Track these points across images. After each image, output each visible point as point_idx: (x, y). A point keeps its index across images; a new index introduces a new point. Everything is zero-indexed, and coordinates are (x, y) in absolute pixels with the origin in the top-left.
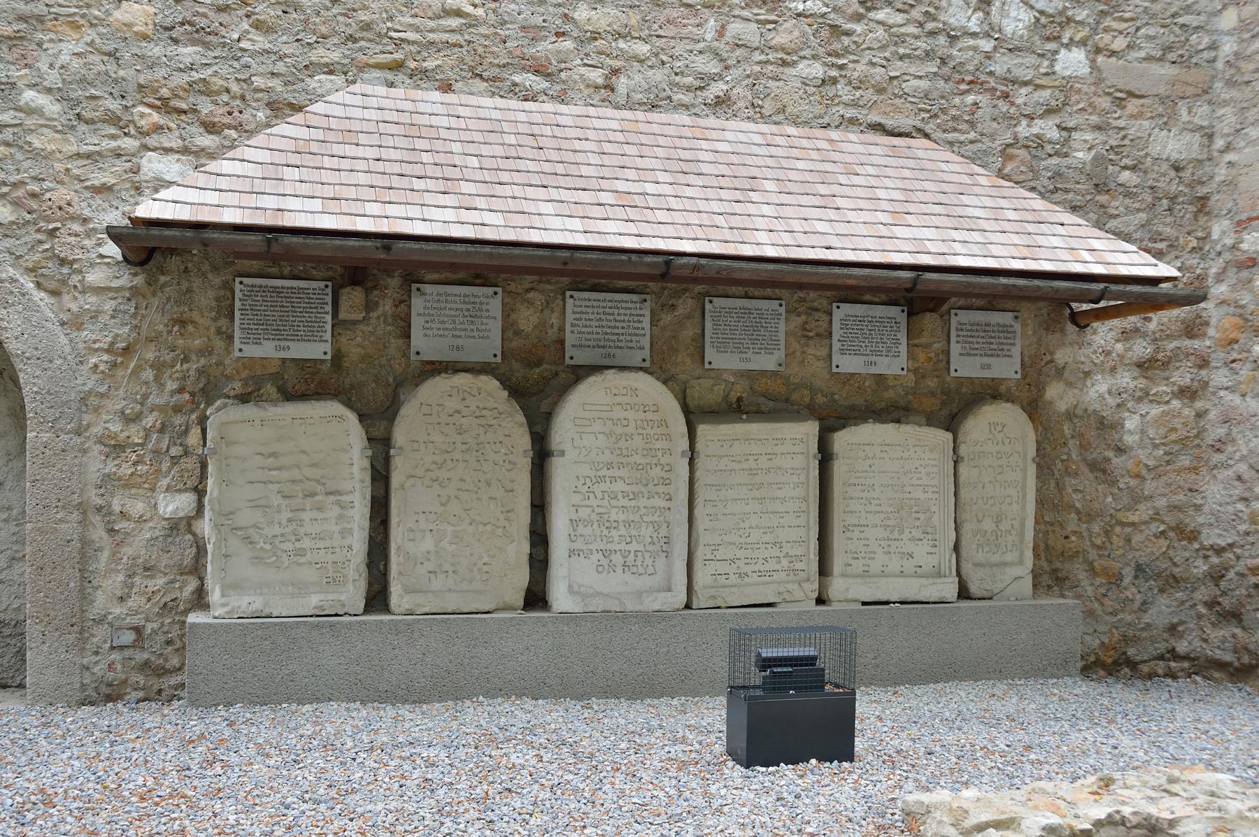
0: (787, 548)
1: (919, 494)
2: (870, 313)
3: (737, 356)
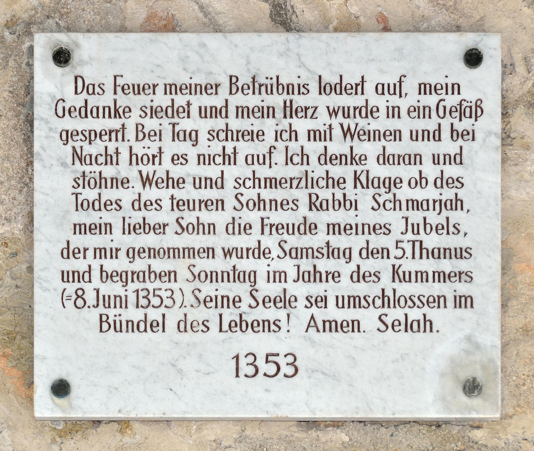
3: (219, 347)
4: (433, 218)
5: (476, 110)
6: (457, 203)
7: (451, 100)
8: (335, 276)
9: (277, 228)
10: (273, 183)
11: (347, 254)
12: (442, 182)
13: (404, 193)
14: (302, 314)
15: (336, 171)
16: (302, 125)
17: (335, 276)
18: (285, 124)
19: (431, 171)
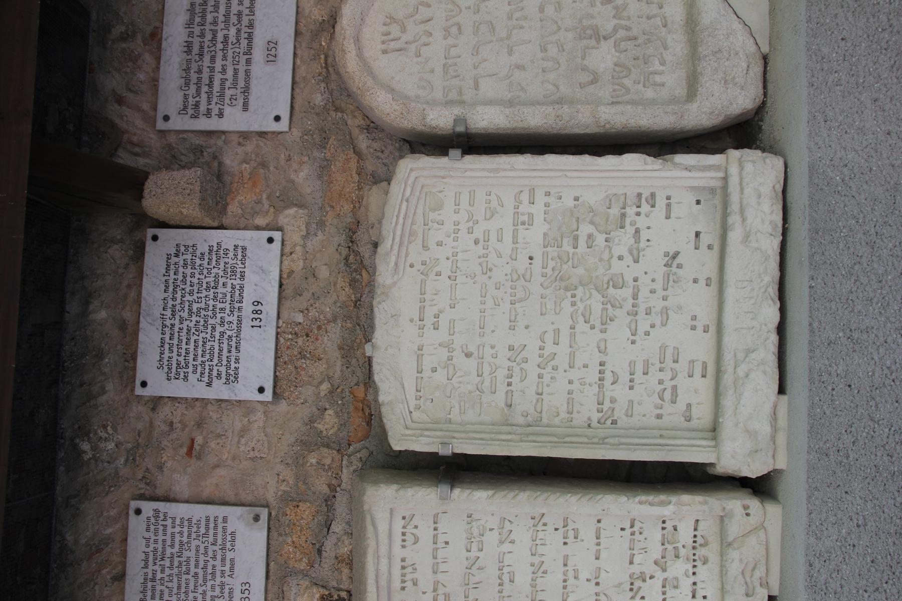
0: (645, 563)
1: (534, 236)
2: (157, 311)
4: (194, 529)
5: (156, 511)
6: (190, 520)
7: (153, 520)
8: (214, 566)
9: (195, 587)
10: (179, 588)
11: (206, 562)
12: (182, 525)
13: (185, 539)
14: (227, 579)
15: (176, 564)
16: (159, 576)
17: (214, 566)
18: (158, 582)
19: (178, 529)
